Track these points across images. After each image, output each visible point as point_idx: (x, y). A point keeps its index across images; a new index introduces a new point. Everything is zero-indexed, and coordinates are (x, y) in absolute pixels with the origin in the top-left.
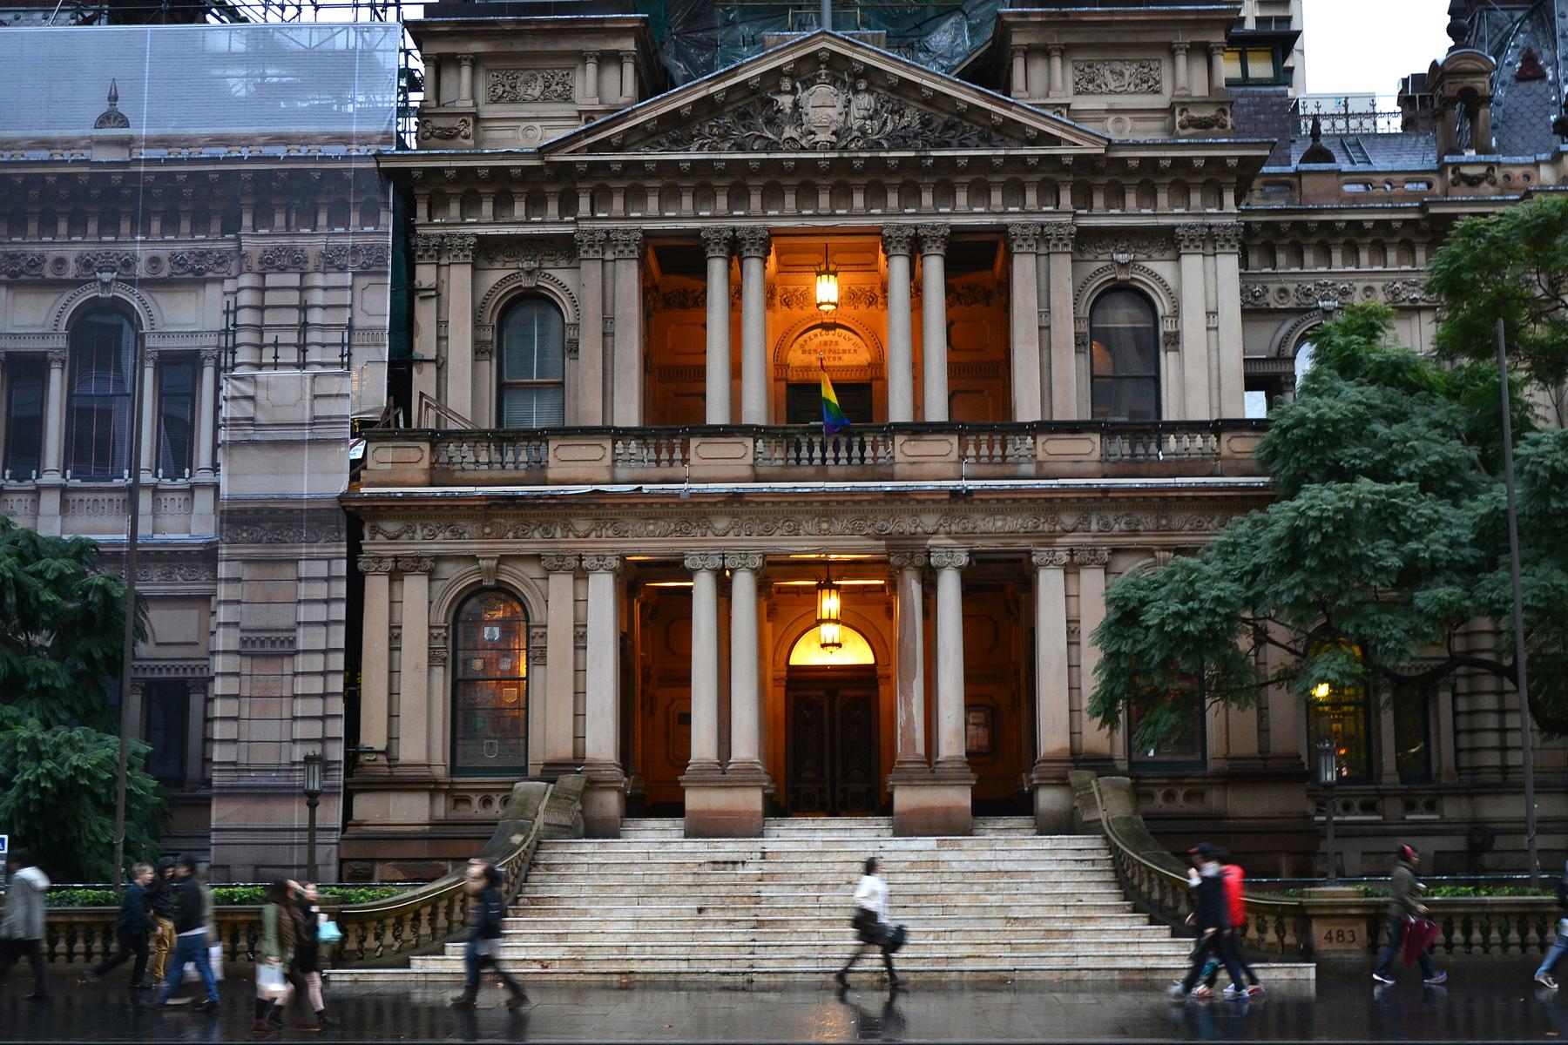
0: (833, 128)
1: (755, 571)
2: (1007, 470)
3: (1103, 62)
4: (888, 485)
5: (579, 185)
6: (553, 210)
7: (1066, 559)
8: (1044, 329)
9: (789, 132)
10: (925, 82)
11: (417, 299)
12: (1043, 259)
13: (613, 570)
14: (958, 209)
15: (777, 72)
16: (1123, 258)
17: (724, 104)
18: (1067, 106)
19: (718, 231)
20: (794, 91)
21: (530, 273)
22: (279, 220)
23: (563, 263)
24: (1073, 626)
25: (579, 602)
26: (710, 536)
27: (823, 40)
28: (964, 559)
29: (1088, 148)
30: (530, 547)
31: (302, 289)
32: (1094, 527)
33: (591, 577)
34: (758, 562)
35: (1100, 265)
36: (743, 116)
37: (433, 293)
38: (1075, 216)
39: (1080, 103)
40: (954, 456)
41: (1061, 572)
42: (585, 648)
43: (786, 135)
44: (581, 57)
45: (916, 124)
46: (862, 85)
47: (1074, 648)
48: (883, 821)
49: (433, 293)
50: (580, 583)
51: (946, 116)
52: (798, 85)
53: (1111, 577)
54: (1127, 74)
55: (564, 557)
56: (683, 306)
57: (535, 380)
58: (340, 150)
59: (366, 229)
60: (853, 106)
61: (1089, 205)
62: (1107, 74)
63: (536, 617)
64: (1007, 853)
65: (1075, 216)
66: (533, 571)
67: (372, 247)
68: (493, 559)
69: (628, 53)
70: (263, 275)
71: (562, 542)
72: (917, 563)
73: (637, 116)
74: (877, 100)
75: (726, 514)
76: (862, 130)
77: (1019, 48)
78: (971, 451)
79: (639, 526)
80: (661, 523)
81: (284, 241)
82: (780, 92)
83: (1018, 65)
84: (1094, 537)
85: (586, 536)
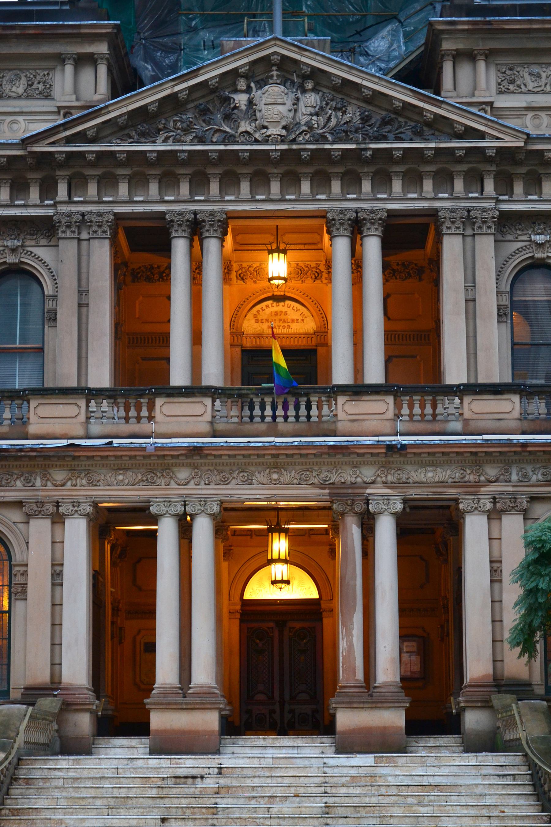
0: (284, 123)
1: (213, 516)
2: (437, 427)
3: (522, 65)
4: (331, 440)
5: (58, 173)
6: (34, 194)
7: (489, 506)
8: (470, 301)
9: (245, 126)
10: (365, 83)
12: (469, 239)
13: (87, 515)
14: (394, 195)
15: (234, 73)
16: (540, 239)
17: (187, 101)
18: (491, 104)
19: (180, 214)
20: (248, 90)
21: (14, 250)
23: (43, 242)
24: (496, 565)
26: (173, 485)
27: (275, 45)
28: (399, 507)
29: (509, 142)
32: (514, 477)
33: (68, 522)
34: (216, 509)
35: (519, 245)
36: (204, 112)
38: (498, 201)
39: (502, 102)
40: (390, 414)
41: (485, 518)
42: (61, 585)
43: (241, 129)
44: (61, 59)
45: (357, 120)
46: (309, 85)
47: (496, 585)
48: (327, 740)
50: (58, 527)
51: (384, 113)
52: (252, 85)
53: (529, 522)
54: (544, 75)
55: (43, 504)
56: (149, 279)
57: (17, 345)
60: (301, 104)
61: (510, 192)
62: (526, 76)
63: (18, 557)
64: (436, 769)
65: (498, 201)
69: (102, 56)
72: (357, 510)
73: (109, 112)
74: (323, 98)
76: (308, 124)
77: (447, 53)
78: (405, 410)
79: (109, 476)
80: (129, 473)
82: (236, 91)
83: (448, 67)
84: (514, 486)
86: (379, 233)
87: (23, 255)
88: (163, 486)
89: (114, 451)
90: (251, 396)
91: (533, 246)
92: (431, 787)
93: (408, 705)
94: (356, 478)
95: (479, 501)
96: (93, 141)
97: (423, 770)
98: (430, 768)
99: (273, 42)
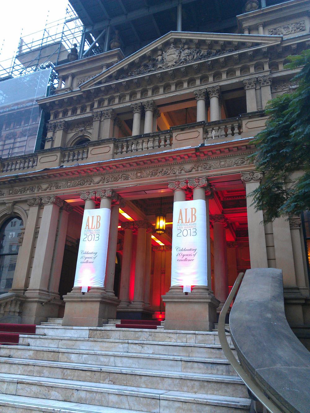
0: (175, 61)
11: (46, 142)
21: (81, 131)
22: (12, 125)
25: (39, 218)
26: (92, 184)
28: (204, 182)
30: (24, 197)
31: (14, 143)
37: (51, 140)
46: (186, 47)
49: (51, 140)
54: (290, 28)
58: (31, 104)
59: (33, 123)
62: (283, 30)
64: (138, 348)
66: (25, 207)
67: (34, 128)
68: (10, 203)
70: (5, 141)
71: (37, 193)
72: (181, 187)
73: (110, 72)
75: (98, 175)
76: (185, 60)
77: (246, 27)
81: (12, 131)
85: (46, 190)
86: (217, 95)
87: (85, 133)
88: (88, 185)
89: (64, 170)
90: (132, 141)
91: (291, 91)
92: (102, 375)
93: (210, 301)
94: (181, 170)
95: (253, 174)
96: (105, 82)
97: (123, 348)
98: (132, 345)
99: (171, 34)
